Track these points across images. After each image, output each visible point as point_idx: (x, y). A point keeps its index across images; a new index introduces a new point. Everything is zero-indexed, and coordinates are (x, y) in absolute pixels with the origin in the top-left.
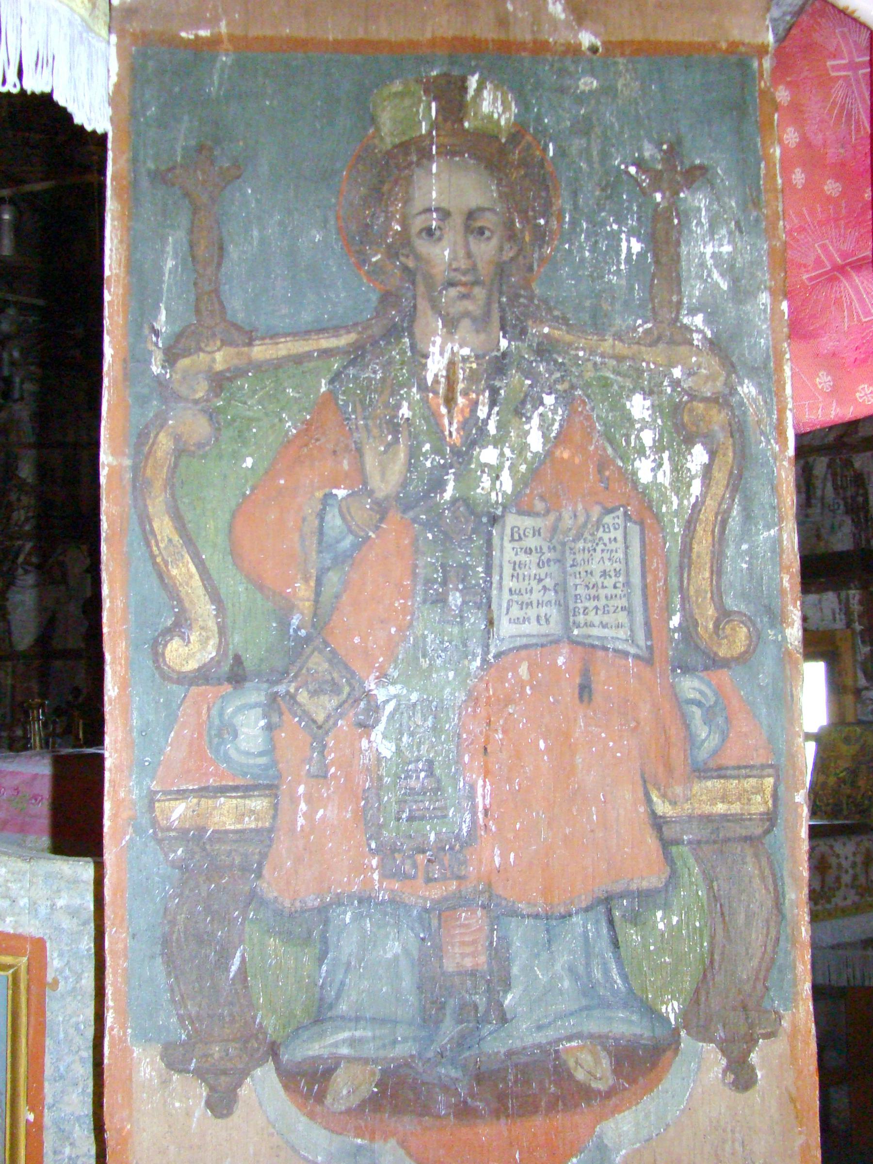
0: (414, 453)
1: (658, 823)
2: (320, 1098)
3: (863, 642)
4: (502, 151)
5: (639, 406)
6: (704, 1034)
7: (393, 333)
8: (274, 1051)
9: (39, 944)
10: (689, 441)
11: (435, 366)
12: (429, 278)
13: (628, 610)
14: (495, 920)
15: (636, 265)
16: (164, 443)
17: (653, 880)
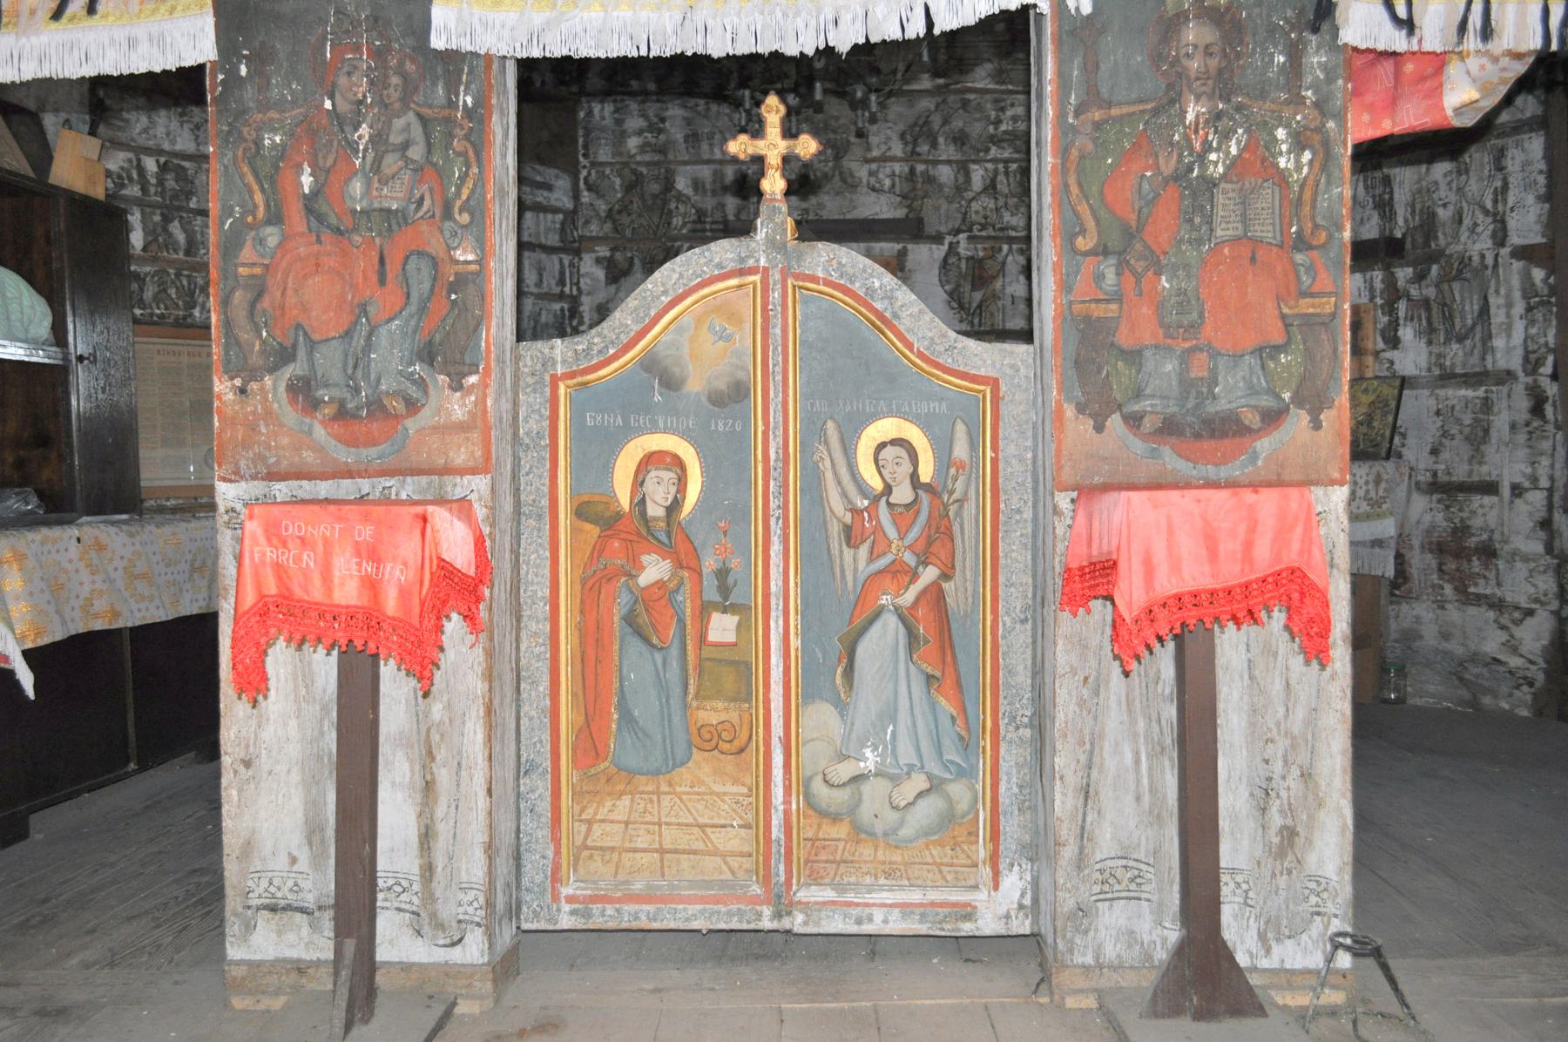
0: (1180, 155)
1: (1283, 317)
2: (1139, 427)
4: (1222, 15)
5: (1281, 133)
6: (1300, 405)
7: (1172, 102)
8: (1120, 407)
9: (996, 381)
10: (1303, 149)
11: (1190, 117)
12: (1188, 77)
13: (1273, 224)
14: (1211, 357)
15: (1282, 67)
16: (1075, 153)
17: (1279, 340)
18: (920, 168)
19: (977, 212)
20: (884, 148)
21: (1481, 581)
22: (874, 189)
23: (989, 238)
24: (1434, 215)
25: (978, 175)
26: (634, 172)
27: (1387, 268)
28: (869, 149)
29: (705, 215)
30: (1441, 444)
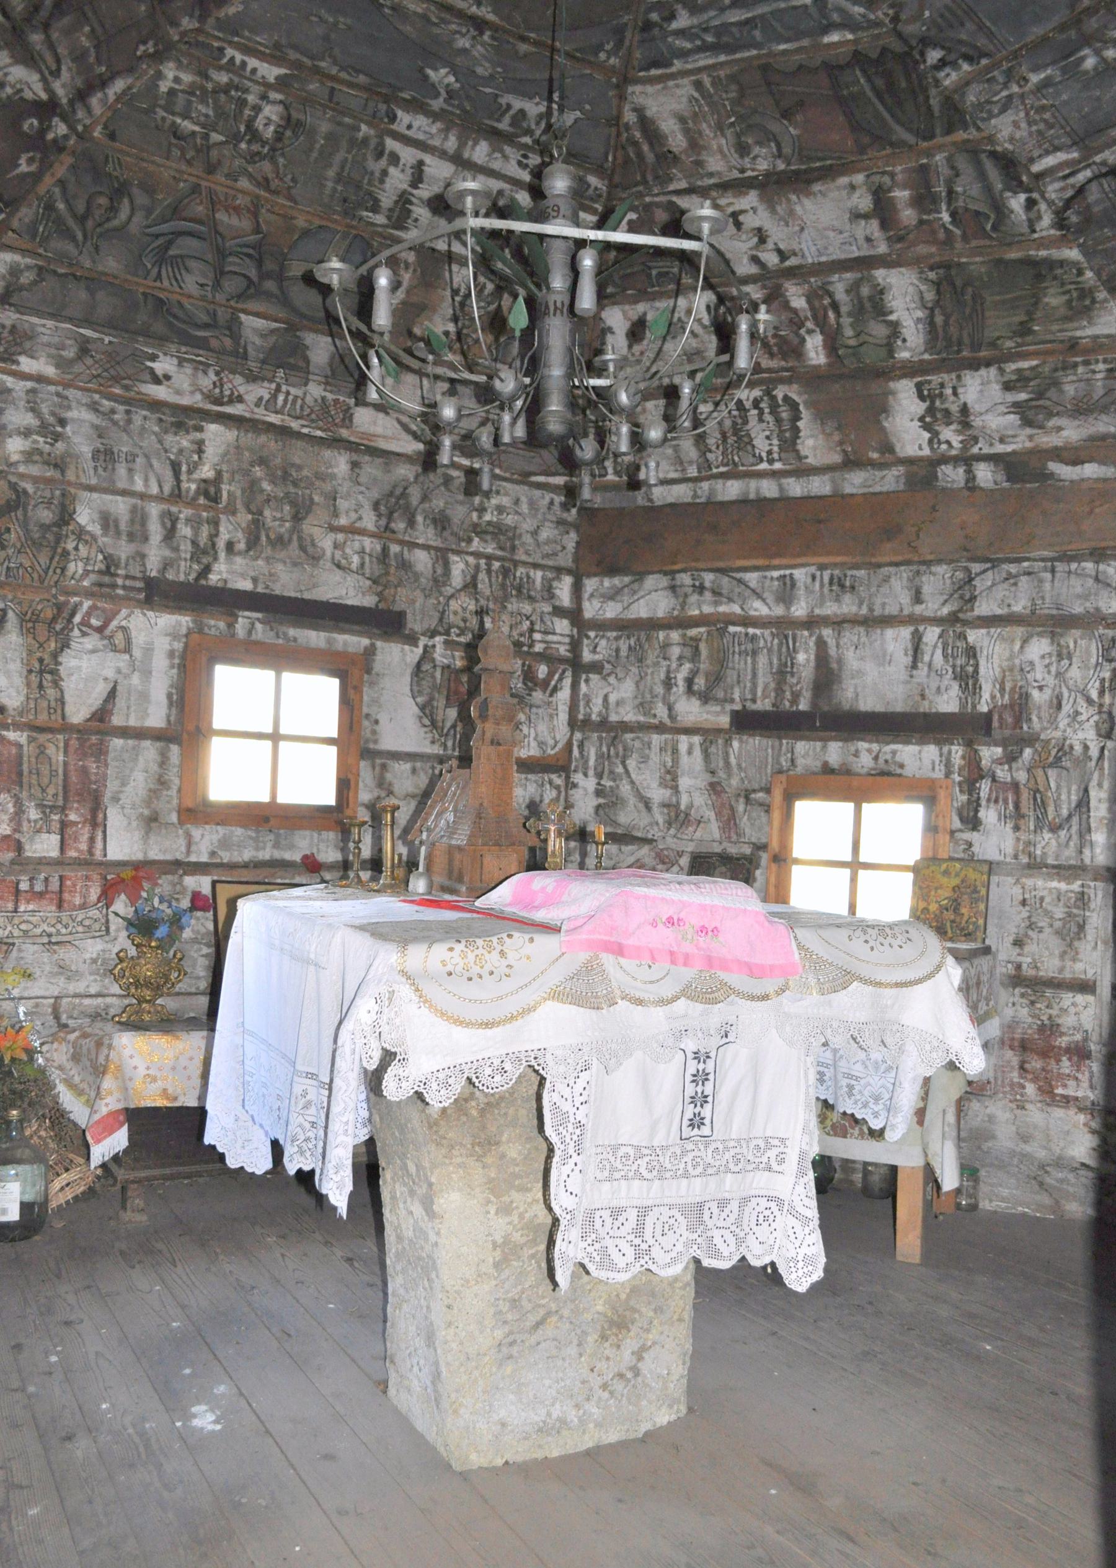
3: (961, 791)
18: (395, 548)
19: (455, 613)
20: (354, 516)
21: (1072, 1083)
22: (339, 566)
24: (1028, 695)
25: (458, 568)
26: (13, 486)
27: (969, 744)
28: (336, 514)
29: (117, 566)
30: (1026, 935)
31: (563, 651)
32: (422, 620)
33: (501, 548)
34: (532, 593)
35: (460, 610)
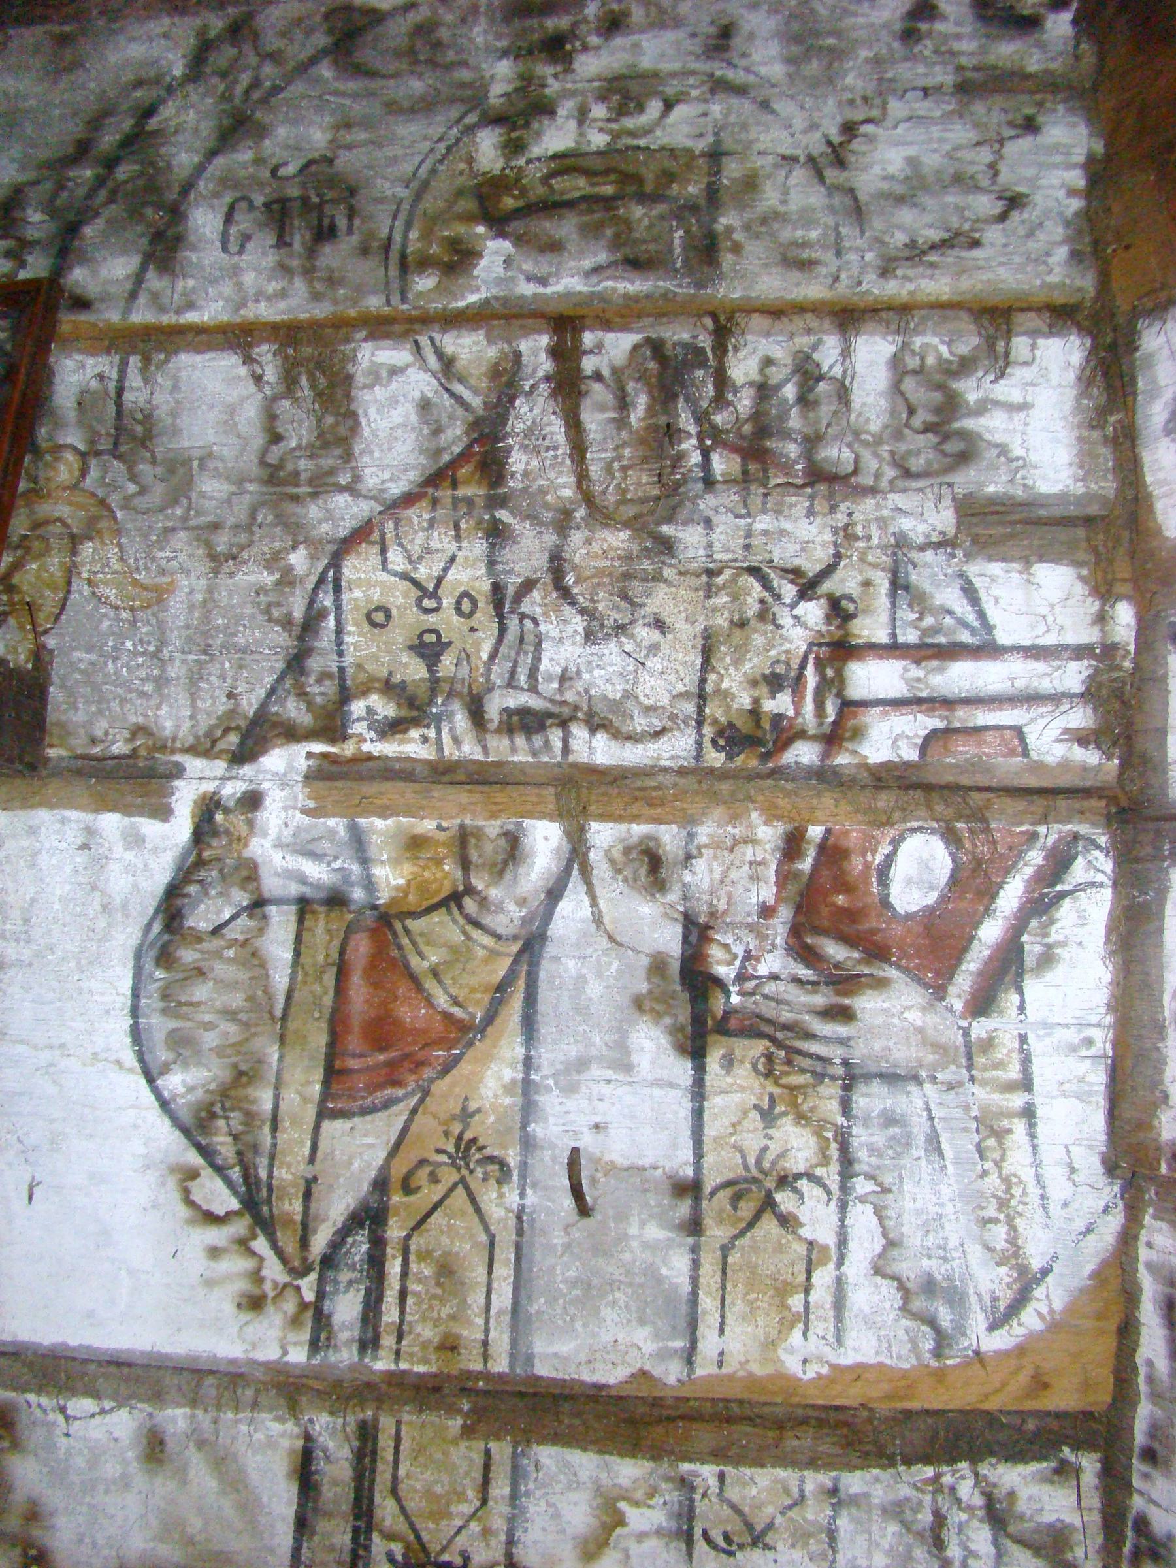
19: (378, 618)
23: (442, 773)
31: (1053, 740)
32: (195, 679)
33: (636, 264)
34: (837, 454)
35: (400, 597)
